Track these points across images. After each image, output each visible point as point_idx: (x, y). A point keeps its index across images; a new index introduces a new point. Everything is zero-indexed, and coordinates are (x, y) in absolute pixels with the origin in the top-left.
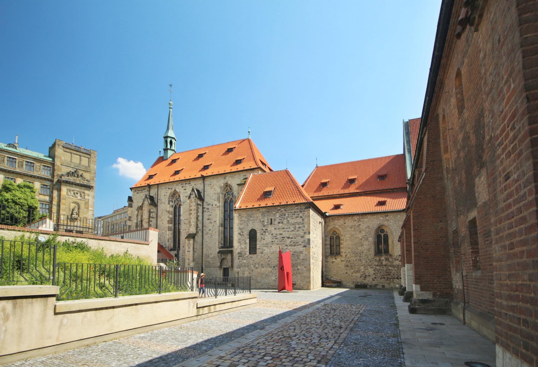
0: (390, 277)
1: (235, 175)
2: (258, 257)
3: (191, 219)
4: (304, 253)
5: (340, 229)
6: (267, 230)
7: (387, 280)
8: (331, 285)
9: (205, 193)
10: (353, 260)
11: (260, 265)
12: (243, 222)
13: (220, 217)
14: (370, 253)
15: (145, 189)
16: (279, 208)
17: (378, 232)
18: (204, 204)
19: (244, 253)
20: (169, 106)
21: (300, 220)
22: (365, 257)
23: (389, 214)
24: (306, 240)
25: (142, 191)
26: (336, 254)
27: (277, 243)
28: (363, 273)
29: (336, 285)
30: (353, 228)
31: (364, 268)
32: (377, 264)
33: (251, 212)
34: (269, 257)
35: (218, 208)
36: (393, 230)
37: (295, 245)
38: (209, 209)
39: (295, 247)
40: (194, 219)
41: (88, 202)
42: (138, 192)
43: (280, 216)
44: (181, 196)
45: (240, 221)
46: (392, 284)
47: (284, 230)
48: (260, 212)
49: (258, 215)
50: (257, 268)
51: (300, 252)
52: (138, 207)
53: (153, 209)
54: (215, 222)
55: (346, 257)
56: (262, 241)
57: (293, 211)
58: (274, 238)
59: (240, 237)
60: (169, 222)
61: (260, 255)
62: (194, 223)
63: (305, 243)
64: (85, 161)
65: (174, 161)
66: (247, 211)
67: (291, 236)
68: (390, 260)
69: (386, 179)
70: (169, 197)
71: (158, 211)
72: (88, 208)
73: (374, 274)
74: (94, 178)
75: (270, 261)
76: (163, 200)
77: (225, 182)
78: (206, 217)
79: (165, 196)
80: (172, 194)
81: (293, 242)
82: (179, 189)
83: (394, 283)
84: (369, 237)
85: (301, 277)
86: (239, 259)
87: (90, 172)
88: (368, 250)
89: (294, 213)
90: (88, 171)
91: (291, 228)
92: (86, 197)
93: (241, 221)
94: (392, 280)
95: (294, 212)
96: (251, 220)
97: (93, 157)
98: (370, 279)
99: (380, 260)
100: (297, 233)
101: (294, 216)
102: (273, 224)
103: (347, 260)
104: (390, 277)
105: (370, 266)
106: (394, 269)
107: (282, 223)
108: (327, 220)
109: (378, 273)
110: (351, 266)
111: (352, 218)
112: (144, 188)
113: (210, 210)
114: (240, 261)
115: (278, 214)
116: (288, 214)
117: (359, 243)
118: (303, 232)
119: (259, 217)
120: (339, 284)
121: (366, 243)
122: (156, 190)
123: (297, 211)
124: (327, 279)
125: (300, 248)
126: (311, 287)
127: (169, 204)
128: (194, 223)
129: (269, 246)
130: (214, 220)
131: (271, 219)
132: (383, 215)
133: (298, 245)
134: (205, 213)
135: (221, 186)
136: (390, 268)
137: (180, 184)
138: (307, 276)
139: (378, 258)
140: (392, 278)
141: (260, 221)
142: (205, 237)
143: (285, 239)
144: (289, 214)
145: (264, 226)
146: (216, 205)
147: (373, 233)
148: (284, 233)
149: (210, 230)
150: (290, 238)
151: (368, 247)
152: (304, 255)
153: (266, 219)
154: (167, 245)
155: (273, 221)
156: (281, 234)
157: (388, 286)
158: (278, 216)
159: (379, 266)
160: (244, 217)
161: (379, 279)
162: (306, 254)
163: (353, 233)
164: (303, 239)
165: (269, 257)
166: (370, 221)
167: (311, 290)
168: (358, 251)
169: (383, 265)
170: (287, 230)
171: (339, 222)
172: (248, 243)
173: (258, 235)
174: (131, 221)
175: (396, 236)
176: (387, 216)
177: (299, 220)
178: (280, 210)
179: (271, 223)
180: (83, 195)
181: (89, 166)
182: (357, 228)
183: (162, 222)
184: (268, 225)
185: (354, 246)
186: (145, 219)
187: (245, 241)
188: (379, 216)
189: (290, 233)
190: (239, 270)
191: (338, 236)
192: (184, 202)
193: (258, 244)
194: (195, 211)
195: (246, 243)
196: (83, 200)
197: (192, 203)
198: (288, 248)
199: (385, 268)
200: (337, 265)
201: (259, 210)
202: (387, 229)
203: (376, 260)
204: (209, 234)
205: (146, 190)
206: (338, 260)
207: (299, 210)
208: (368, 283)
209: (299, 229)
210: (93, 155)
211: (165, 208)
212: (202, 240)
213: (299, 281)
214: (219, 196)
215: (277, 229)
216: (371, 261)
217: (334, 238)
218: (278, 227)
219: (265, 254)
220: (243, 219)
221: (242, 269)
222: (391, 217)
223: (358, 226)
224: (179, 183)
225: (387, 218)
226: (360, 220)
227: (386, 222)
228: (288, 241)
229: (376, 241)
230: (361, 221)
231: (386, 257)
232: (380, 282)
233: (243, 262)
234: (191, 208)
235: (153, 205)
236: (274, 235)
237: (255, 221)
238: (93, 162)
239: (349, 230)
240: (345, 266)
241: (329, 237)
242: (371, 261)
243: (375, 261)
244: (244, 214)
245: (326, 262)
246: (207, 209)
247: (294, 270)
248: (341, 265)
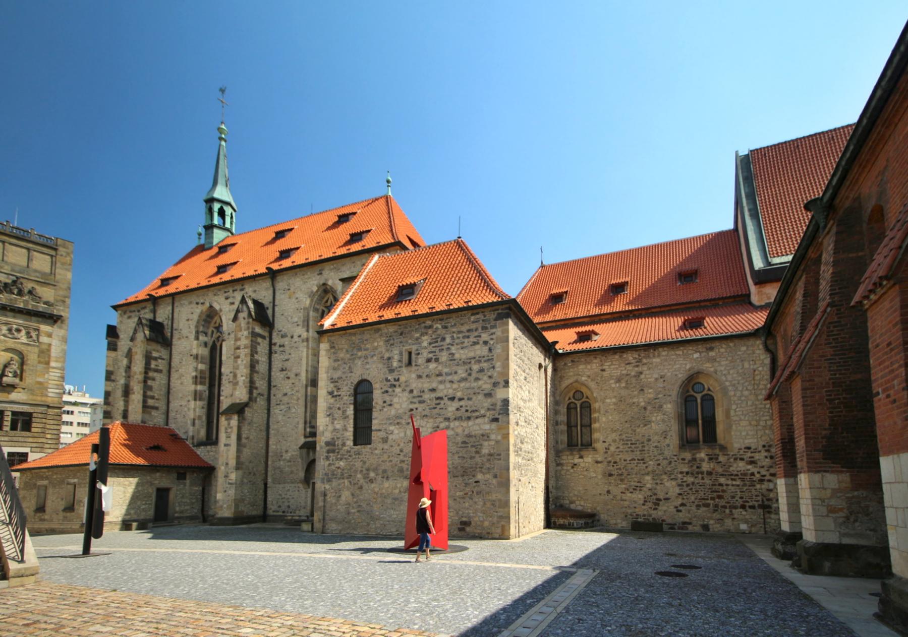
0: (722, 502)
1: (343, 265)
2: (376, 452)
3: (237, 369)
4: (493, 437)
5: (592, 385)
6: (398, 380)
7: (715, 511)
8: (569, 524)
9: (276, 309)
10: (625, 460)
11: (380, 471)
12: (339, 363)
13: (310, 364)
14: (667, 441)
15: (145, 308)
17: (688, 391)
18: (274, 334)
19: (340, 442)
20: (219, 135)
21: (481, 350)
22: (656, 453)
23: (717, 343)
24: (499, 404)
26: (582, 445)
27: (424, 413)
28: (649, 493)
29: (582, 521)
30: (622, 381)
31: (654, 479)
32: (685, 470)
33: (359, 337)
34: (401, 451)
35: (305, 344)
36: (727, 383)
37: (469, 418)
38: (283, 346)
39: (470, 423)
40: (246, 367)
41: (49, 350)
42: (130, 314)
43: (430, 344)
46: (728, 522)
47: (440, 378)
48: (381, 335)
49: (376, 344)
50: (371, 481)
51: (483, 435)
53: (158, 352)
55: (606, 452)
56: (385, 410)
58: (415, 400)
59: (332, 401)
60: (196, 381)
61: (380, 446)
62: (244, 378)
63: (494, 410)
64: (41, 262)
65: (223, 249)
66: (351, 334)
67: (459, 395)
68: (722, 459)
69: (698, 281)
70: (198, 322)
71: (173, 357)
72: (48, 363)
73: (680, 494)
74: (67, 300)
75: (403, 461)
76: (185, 332)
77: (321, 283)
78: (277, 364)
80: (204, 317)
81: (463, 409)
82: (219, 304)
83: (734, 518)
84: (664, 403)
85: (485, 504)
86: (327, 458)
87: (55, 285)
88: (662, 434)
90: (49, 284)
91: (460, 372)
92: (44, 339)
93: (335, 361)
94: (727, 511)
96: (360, 358)
97: (64, 254)
98: (668, 507)
99: (694, 459)
100: (475, 384)
101: (466, 340)
102: (413, 364)
103: (610, 459)
104: (722, 502)
105: (669, 474)
106: (734, 483)
107: (437, 360)
108: (561, 364)
109: (690, 492)
110: (621, 475)
111: (621, 356)
112: (143, 305)
114: (330, 465)
116: (452, 337)
117: (638, 418)
118: (489, 381)
119: (379, 350)
120: (590, 521)
121: (657, 417)
122: (170, 308)
124: (561, 506)
125: (483, 426)
126: (513, 531)
127: (197, 338)
129: (403, 422)
131: (410, 353)
132: (700, 347)
133: (477, 418)
134: (276, 355)
135: (312, 292)
136: (722, 480)
137: (222, 292)
138: (500, 500)
139: (688, 455)
140: (728, 505)
141: (382, 357)
142: (275, 411)
143: (442, 402)
144: (455, 335)
145: (391, 371)
147: (675, 391)
148: (441, 387)
150: (456, 400)
151: (662, 427)
152: (493, 443)
154: (191, 434)
155: (413, 356)
156: (433, 390)
157: (718, 526)
158: (425, 344)
159: (692, 474)
160: (342, 349)
161: (694, 508)
162: (497, 442)
163: (624, 393)
164: (489, 400)
165: (401, 451)
166: (666, 363)
167: (513, 540)
168: (637, 438)
169: (702, 473)
170: (449, 378)
171: (589, 367)
172: (352, 417)
173: (377, 395)
174: (113, 381)
175: (736, 398)
176: (711, 349)
177: (481, 350)
179: (410, 363)
180: (34, 334)
181: (52, 273)
182: (633, 380)
183: (179, 382)
184: (400, 367)
185: (627, 425)
186: (135, 373)
187: (344, 412)
188: (690, 349)
189: (455, 386)
190: (327, 487)
191: (585, 402)
192: (229, 334)
193: (376, 418)
194: (248, 351)
195: (346, 417)
196: (34, 345)
197: (241, 330)
198: (452, 425)
199: (707, 481)
200: (585, 473)
201: (379, 330)
202: (711, 382)
203: (683, 459)
205: (147, 311)
206: (586, 459)
208: (664, 518)
209: (480, 375)
210: (64, 250)
212: (265, 419)
213: (479, 514)
214: (308, 316)
215: (424, 376)
216: (670, 463)
217: (576, 408)
218: (427, 371)
219: (393, 444)
220: (341, 355)
221: (335, 483)
222: (722, 350)
223: (635, 376)
224: (220, 290)
225: (712, 354)
226: (640, 361)
227: (708, 365)
228: (452, 407)
229: (681, 413)
230: (646, 364)
231: (710, 452)
232: (696, 515)
233: (337, 465)
234: (238, 343)
235: (157, 342)
236: (415, 392)
237: (369, 360)
238: (63, 264)
239: (613, 386)
240: (604, 474)
241: (566, 407)
242: (670, 463)
243: (681, 461)
245: (558, 465)
246: (280, 346)
247: (467, 484)
248: (595, 472)
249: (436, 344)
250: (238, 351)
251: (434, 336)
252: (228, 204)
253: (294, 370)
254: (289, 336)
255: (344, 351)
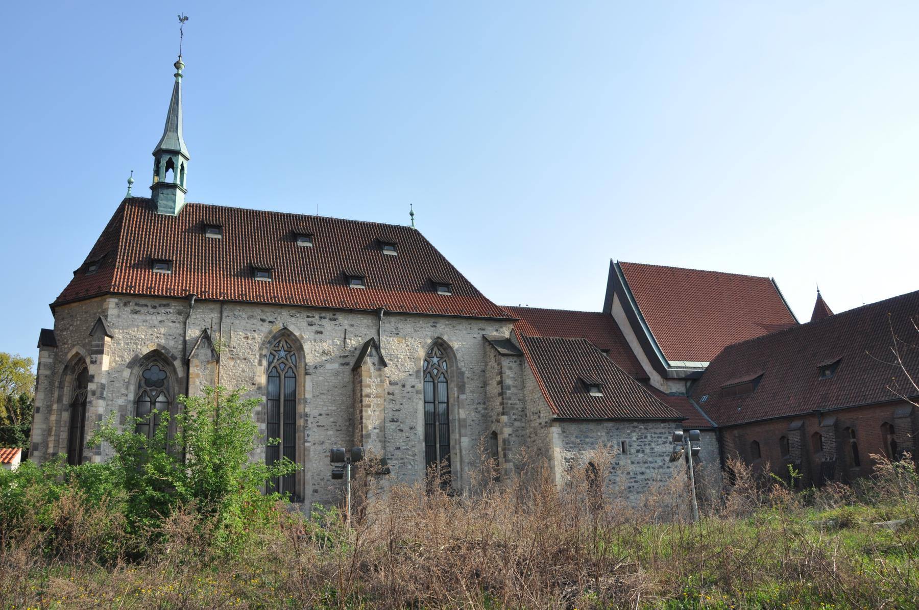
1: (460, 324)
3: (369, 417)
6: (618, 464)
16: (635, 424)
25: (154, 307)
43: (638, 439)
44: (307, 347)
45: (564, 443)
47: (647, 465)
52: (137, 356)
54: (411, 428)
57: (658, 431)
58: (631, 480)
62: (377, 431)
70: (263, 344)
77: (436, 336)
79: (247, 338)
89: (660, 435)
91: (658, 461)
93: (567, 443)
95: (660, 433)
101: (660, 440)
102: (628, 453)
107: (643, 451)
113: (398, 396)
115: (634, 434)
123: (663, 431)
127: (260, 364)
128: (377, 431)
130: (409, 422)
135: (426, 343)
137: (304, 314)
146: (413, 387)
148: (648, 471)
149: (399, 448)
153: (615, 442)
156: (642, 473)
158: (634, 439)
170: (652, 465)
178: (637, 427)
179: (624, 451)
189: (656, 471)
204: (396, 459)
207: (667, 430)
211: (248, 373)
244: (573, 428)
249: (642, 440)
250: (367, 399)
251: (640, 434)
252: (187, 159)
253: (409, 422)
254: (400, 384)
255: (574, 436)
